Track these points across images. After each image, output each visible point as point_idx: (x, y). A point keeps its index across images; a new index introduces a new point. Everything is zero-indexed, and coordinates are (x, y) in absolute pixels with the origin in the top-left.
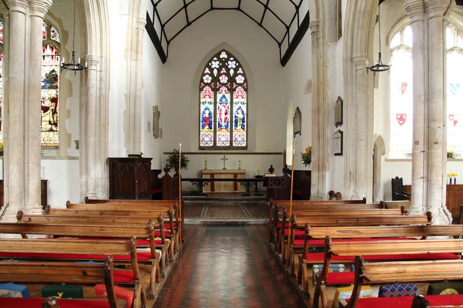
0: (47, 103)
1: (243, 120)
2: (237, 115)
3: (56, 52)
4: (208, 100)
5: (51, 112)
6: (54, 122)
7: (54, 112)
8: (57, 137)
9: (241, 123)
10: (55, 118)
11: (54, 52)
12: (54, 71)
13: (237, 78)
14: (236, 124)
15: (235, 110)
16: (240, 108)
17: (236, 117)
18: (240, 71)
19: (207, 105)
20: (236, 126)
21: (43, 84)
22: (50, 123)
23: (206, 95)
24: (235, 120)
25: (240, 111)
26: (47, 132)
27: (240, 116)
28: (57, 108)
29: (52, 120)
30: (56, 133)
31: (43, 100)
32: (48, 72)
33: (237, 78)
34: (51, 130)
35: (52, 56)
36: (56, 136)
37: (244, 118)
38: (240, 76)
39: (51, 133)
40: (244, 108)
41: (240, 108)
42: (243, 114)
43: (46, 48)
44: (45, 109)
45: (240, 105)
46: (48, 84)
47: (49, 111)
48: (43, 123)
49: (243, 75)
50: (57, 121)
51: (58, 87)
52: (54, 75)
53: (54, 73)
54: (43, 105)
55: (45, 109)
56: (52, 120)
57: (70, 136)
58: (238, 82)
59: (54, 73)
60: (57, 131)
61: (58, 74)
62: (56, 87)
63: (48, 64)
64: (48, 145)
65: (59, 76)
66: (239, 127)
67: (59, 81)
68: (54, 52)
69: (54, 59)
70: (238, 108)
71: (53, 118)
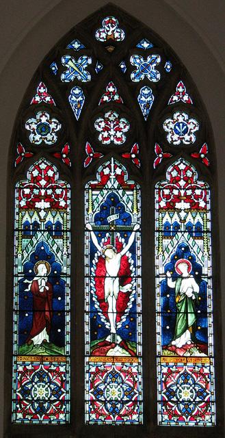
1: (199, 304)
2: (171, 284)
4: (195, 219)
9: (191, 319)
14: (170, 320)
15: (161, 264)
16: (183, 252)
17: (167, 290)
18: (181, 95)
19: (183, 238)
20: (171, 334)
23: (178, 199)
24: (166, 306)
25: (183, 268)
27: (189, 286)
33: (168, 125)
37: (202, 294)
38: (180, 117)
40: (201, 250)
41: (183, 252)
42: (198, 279)
45: (183, 238)
49: (193, 110)
58: (172, 138)
66: (184, 339)
70: (173, 250)
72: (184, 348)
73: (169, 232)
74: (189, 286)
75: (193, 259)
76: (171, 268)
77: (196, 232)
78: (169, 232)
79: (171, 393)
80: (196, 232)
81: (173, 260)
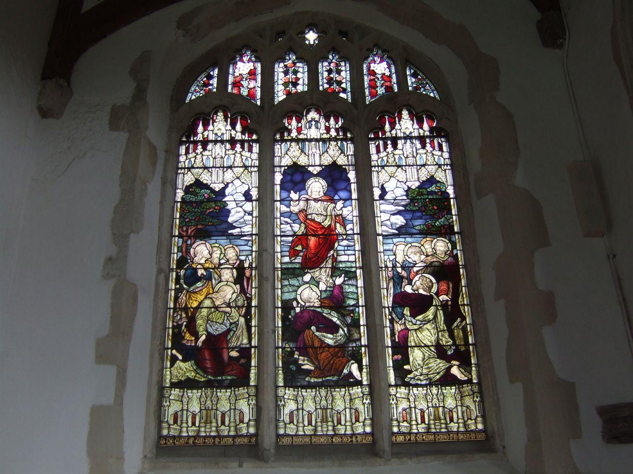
0: (419, 285)
3: (432, 130)
5: (441, 314)
6: (457, 351)
7: (452, 313)
8: (472, 407)
10: (459, 333)
11: (426, 126)
12: (432, 180)
21: (400, 220)
22: (440, 351)
26: (434, 390)
28: (464, 299)
29: (446, 340)
30: (467, 388)
31: (404, 274)
32: (415, 185)
34: (447, 380)
35: (422, 139)
36: (468, 401)
39: (450, 391)
43: (400, 119)
44: (419, 304)
46: (418, 222)
47: (432, 309)
48: (416, 355)
50: (467, 344)
51: (456, 229)
52: (432, 193)
53: (433, 188)
54: (408, 289)
55: (419, 304)
56: (446, 340)
57: (568, 390)
59: (433, 188)
60: (469, 381)
61: (450, 191)
62: (446, 232)
63: (410, 161)
64: (442, 438)
65: (452, 196)
67: (454, 211)
68: (426, 126)
69: (428, 146)
71: (452, 336)
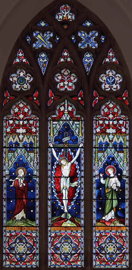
1: (120, 193)
2: (102, 181)
9: (115, 203)
13: (103, 78)
14: (102, 204)
16: (111, 161)
17: (100, 185)
18: (111, 58)
20: (102, 212)
24: (99, 195)
27: (114, 182)
33: (103, 78)
37: (123, 187)
40: (121, 158)
41: (111, 161)
42: (120, 178)
45: (111, 152)
49: (120, 67)
66: (111, 215)
72: (110, 221)
73: (102, 148)
74: (114, 182)
75: (117, 166)
76: (103, 171)
77: (30, 148)
78: (102, 148)
79: (101, 248)
80: (30, 148)
81: (104, 166)
